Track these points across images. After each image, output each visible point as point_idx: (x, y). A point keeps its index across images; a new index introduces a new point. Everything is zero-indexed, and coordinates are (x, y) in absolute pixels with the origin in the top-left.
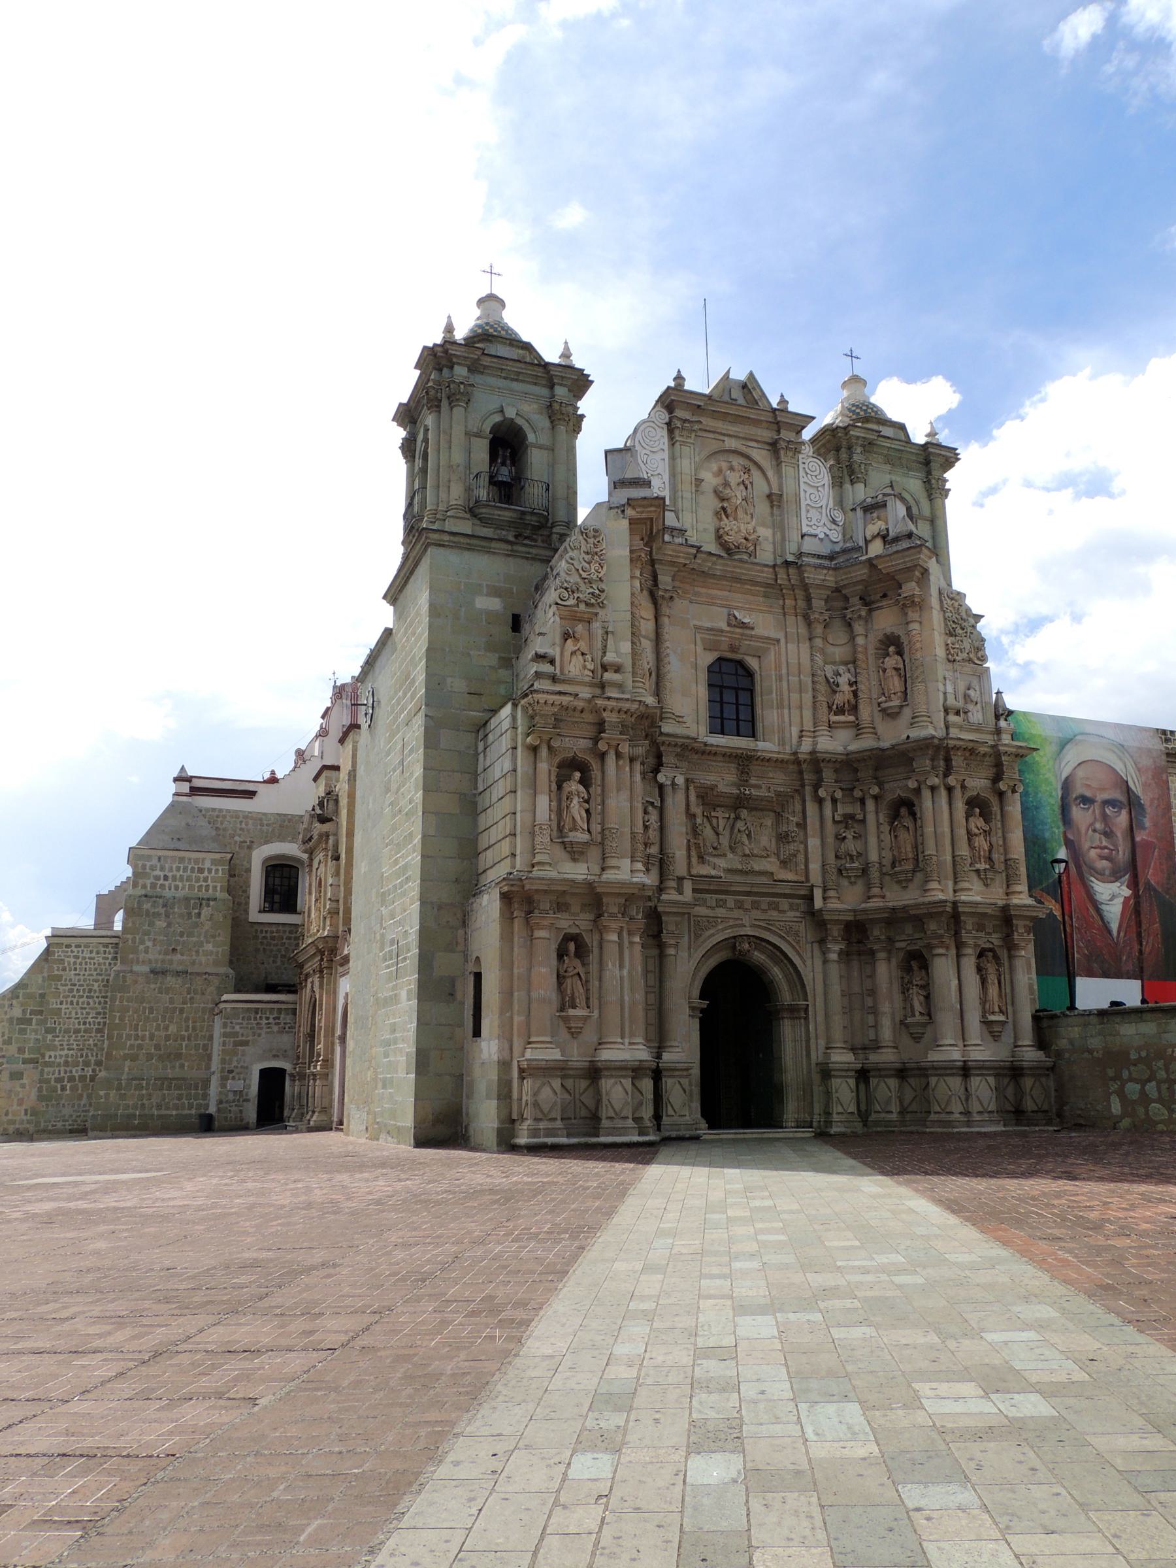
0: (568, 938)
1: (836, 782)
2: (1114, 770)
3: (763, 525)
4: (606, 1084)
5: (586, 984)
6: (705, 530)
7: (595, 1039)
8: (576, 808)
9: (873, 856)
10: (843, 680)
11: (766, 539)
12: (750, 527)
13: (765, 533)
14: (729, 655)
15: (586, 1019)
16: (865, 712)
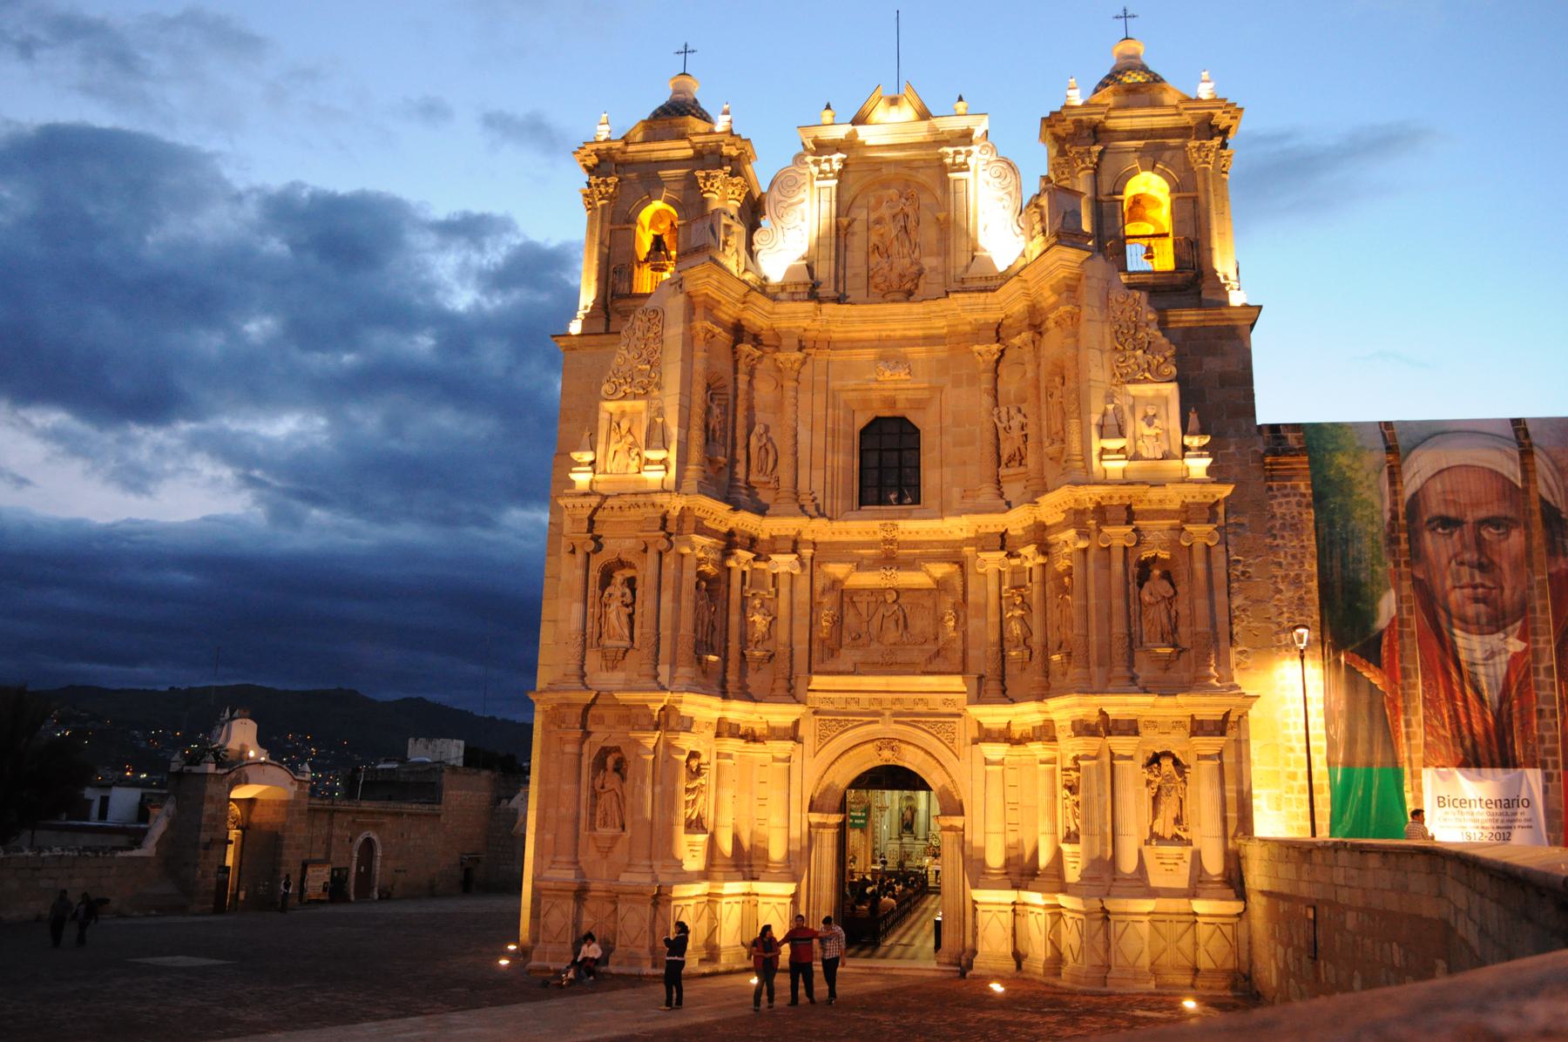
0: (605, 752)
1: (1002, 548)
2: (1502, 476)
3: (931, 255)
4: (622, 909)
5: (621, 801)
6: (855, 275)
7: (626, 860)
8: (615, 616)
9: (1036, 638)
10: (1015, 424)
11: (933, 269)
12: (907, 261)
13: (929, 262)
14: (887, 413)
15: (614, 839)
16: (1031, 460)
